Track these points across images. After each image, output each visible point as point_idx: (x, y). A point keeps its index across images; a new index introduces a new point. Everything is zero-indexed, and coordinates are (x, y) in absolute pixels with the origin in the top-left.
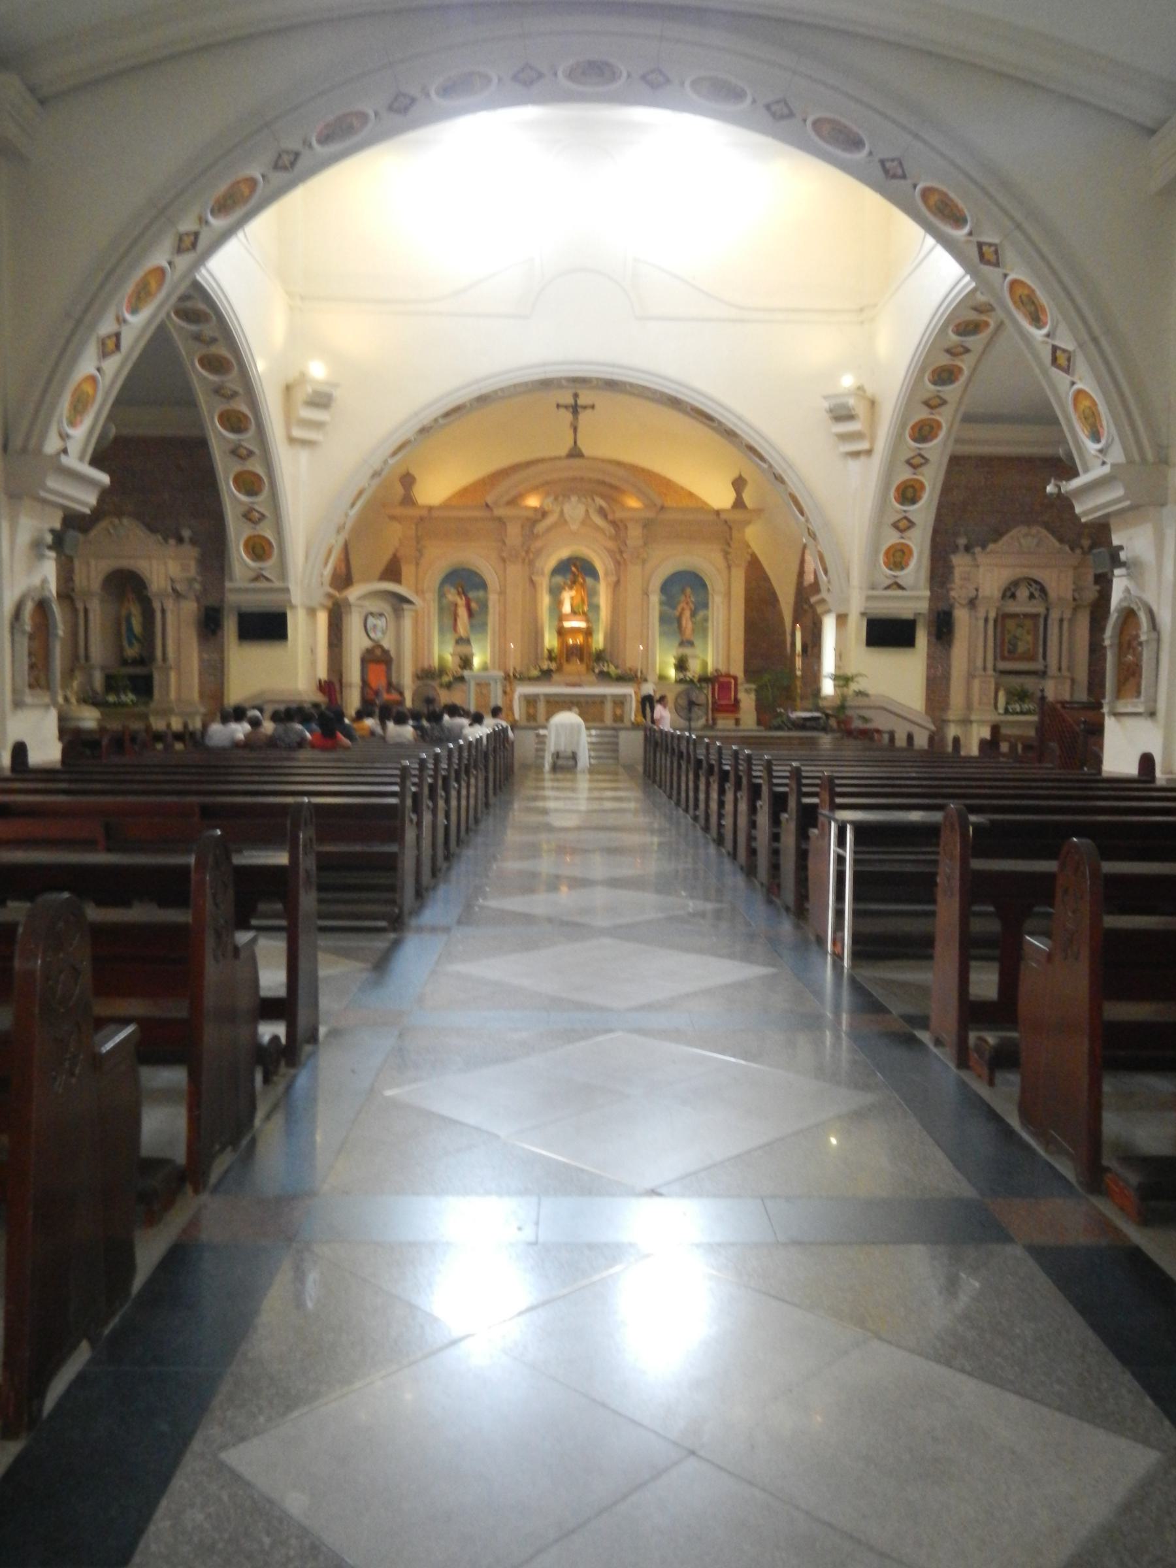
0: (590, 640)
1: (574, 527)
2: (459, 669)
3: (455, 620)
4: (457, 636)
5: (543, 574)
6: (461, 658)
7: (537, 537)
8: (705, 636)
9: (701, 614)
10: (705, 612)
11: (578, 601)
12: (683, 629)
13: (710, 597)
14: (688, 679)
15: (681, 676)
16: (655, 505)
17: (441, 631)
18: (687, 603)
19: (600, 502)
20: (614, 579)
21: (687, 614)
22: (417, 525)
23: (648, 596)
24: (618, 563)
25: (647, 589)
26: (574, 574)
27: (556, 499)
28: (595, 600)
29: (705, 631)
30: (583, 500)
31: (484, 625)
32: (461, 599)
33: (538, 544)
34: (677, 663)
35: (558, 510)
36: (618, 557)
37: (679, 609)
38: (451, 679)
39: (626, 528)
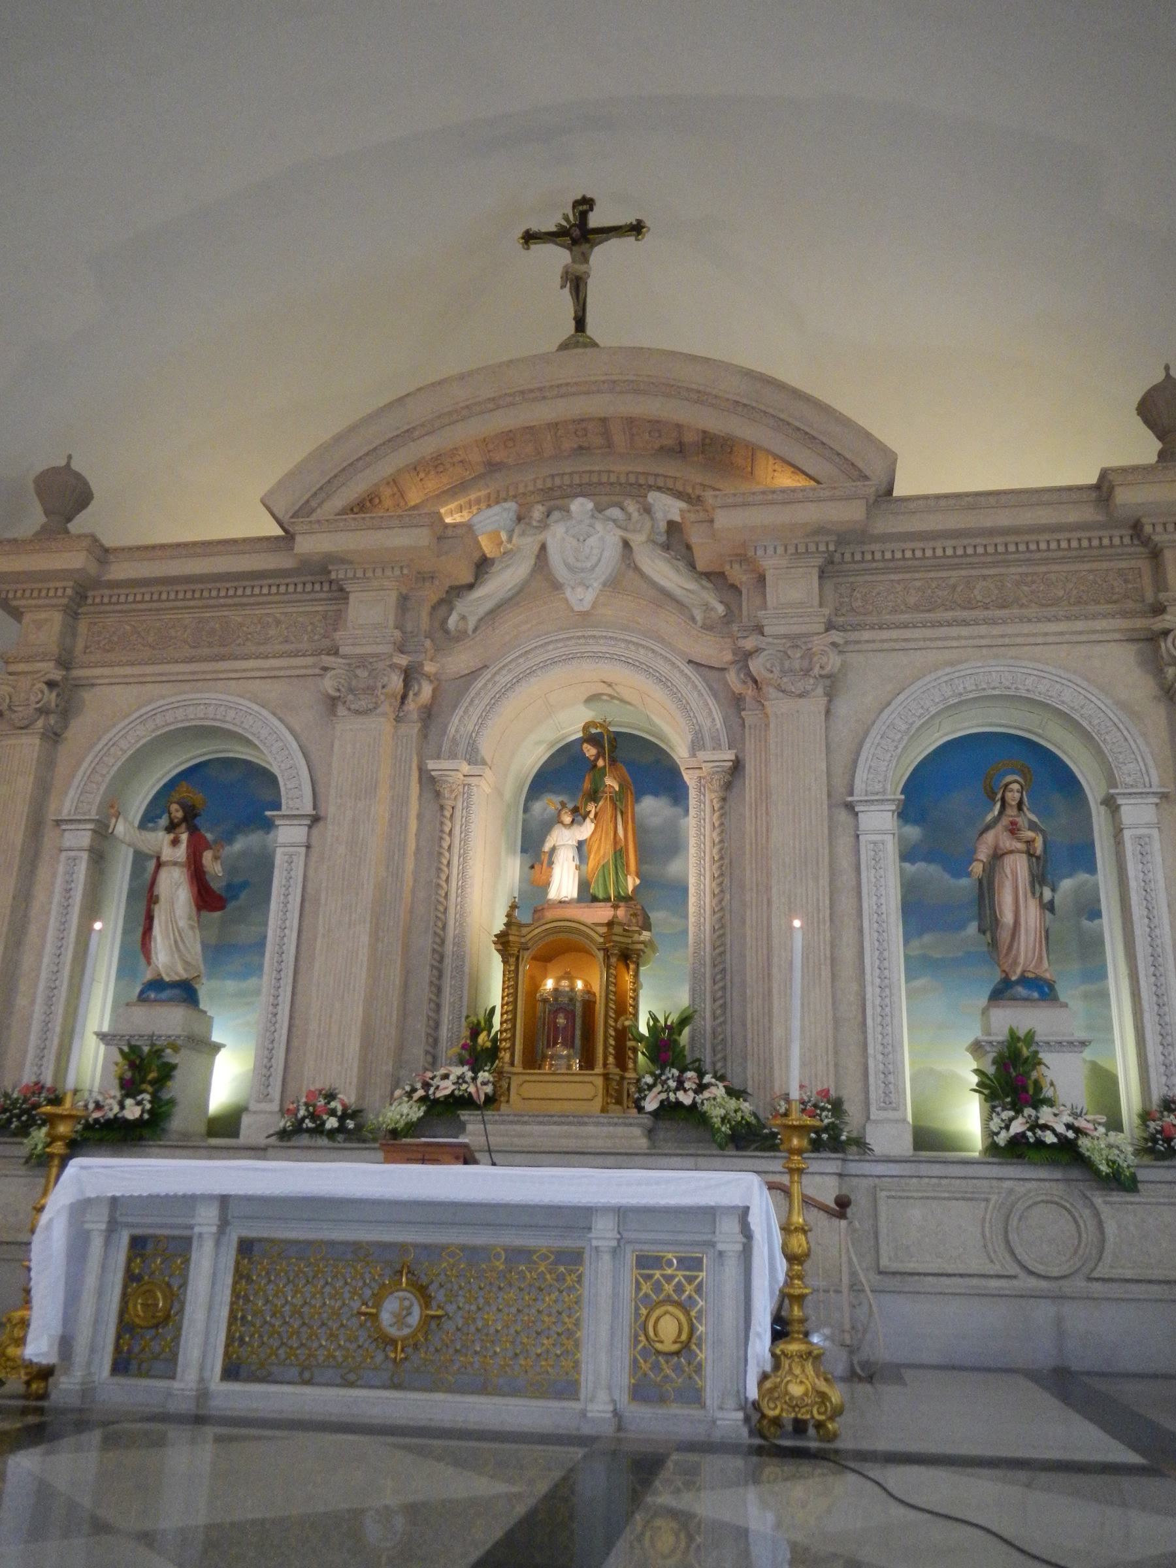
0: (628, 978)
1: (582, 598)
4: (149, 976)
5: (473, 757)
7: (461, 636)
8: (1096, 973)
9: (1066, 884)
10: (1083, 877)
11: (602, 852)
12: (1004, 936)
13: (1099, 818)
14: (1050, 1138)
15: (1017, 1127)
16: (866, 478)
17: (126, 969)
18: (1013, 830)
19: (668, 507)
20: (730, 755)
21: (1017, 868)
23: (850, 807)
25: (851, 794)
27: (519, 519)
28: (673, 868)
29: (1092, 947)
30: (615, 512)
32: (175, 842)
33: (459, 661)
34: (991, 1070)
35: (528, 544)
37: (983, 853)
39: (762, 579)
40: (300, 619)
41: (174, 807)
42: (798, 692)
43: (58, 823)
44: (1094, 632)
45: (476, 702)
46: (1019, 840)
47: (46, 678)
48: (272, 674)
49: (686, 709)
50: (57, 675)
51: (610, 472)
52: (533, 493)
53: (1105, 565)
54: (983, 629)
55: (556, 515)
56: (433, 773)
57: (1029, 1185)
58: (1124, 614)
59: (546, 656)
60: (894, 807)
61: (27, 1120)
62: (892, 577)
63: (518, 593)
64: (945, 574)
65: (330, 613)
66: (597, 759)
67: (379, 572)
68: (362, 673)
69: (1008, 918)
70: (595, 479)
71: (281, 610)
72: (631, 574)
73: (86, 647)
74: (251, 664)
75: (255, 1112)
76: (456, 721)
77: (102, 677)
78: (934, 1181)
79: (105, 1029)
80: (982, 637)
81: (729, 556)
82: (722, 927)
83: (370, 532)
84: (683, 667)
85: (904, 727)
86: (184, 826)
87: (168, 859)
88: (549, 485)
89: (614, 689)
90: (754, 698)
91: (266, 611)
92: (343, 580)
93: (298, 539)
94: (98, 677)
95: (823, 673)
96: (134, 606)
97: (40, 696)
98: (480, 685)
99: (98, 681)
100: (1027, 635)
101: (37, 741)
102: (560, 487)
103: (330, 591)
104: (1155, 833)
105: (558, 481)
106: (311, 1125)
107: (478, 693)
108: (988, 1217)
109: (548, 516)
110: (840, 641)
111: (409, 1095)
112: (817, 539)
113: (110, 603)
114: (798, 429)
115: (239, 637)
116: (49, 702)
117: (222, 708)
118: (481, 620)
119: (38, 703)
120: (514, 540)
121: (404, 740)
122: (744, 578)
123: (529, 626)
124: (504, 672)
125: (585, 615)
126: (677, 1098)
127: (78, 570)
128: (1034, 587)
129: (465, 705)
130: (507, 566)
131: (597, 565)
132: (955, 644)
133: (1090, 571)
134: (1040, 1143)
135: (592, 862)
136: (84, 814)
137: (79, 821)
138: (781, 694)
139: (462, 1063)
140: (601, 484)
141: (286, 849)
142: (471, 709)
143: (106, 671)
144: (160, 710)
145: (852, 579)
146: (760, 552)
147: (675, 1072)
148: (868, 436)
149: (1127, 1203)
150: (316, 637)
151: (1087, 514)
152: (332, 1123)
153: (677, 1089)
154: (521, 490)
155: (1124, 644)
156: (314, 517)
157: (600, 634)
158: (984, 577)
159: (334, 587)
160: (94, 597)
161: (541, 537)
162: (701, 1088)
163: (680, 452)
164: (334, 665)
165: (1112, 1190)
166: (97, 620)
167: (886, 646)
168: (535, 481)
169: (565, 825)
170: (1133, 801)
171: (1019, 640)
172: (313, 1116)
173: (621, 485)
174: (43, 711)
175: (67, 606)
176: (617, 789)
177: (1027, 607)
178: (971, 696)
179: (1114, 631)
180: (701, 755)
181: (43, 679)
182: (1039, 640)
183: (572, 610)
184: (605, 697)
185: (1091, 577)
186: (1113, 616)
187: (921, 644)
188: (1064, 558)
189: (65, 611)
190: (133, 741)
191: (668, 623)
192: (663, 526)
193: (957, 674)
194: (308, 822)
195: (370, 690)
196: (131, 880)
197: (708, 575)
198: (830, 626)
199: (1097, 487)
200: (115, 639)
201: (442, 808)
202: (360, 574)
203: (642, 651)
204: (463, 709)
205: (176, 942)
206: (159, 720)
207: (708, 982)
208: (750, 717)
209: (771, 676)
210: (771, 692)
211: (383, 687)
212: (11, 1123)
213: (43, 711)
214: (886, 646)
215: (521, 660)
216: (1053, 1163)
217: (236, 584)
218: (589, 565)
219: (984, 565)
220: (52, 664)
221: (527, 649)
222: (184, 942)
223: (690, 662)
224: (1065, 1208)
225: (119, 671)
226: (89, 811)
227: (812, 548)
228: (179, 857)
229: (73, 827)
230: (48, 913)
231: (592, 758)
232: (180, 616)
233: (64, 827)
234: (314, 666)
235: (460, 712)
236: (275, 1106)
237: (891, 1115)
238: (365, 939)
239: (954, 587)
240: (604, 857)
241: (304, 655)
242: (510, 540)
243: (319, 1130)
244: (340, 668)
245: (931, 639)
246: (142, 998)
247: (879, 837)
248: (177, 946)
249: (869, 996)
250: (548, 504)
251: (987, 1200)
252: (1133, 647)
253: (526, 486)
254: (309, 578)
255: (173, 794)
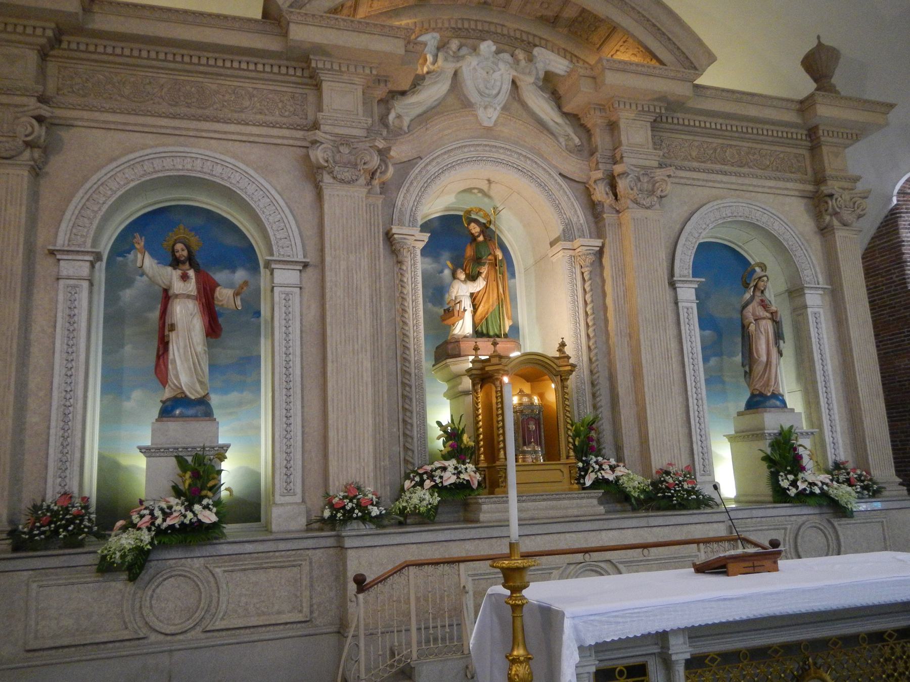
2: (178, 507)
3: (164, 345)
4: (168, 394)
6: (181, 461)
12: (758, 369)
14: (817, 491)
20: (598, 243)
22: (44, 56)
24: (594, 209)
26: (474, 238)
31: (250, 362)
32: (185, 277)
33: (401, 151)
34: (769, 451)
35: (450, 67)
36: (601, 193)
38: (146, 537)
39: (613, 126)
40: (270, 96)
41: (179, 246)
42: (648, 205)
43: (52, 253)
44: (787, 189)
45: (415, 184)
46: (767, 311)
47: (36, 113)
48: (252, 139)
49: (558, 207)
50: (45, 111)
51: (503, 25)
52: (447, 29)
53: (788, 150)
54: (733, 179)
55: (464, 51)
56: (396, 236)
57: (805, 518)
58: (802, 182)
59: (462, 156)
60: (697, 286)
61: (74, 528)
62: (683, 137)
63: (438, 105)
64: (710, 140)
65: (297, 95)
66: (478, 236)
67: (352, 69)
68: (345, 150)
69: (764, 358)
70: (493, 28)
71: (254, 86)
72: (516, 104)
73: (58, 89)
74: (232, 128)
75: (282, 505)
76: (402, 198)
77: (82, 119)
78: (759, 519)
79: (148, 443)
80: (732, 183)
81: (595, 104)
82: (597, 360)
83: (356, 34)
84: (557, 178)
85: (697, 235)
86: (188, 263)
87: (181, 292)
88: (460, 26)
89: (489, 187)
90: (611, 206)
91: (241, 84)
92: (321, 69)
93: (292, 27)
94: (76, 119)
95: (663, 194)
96: (111, 58)
97: (30, 129)
98: (417, 171)
99: (76, 123)
100: (755, 186)
101: (26, 173)
102: (467, 29)
103: (303, 77)
104: (821, 311)
105: (466, 25)
106: (360, 514)
107: (416, 178)
108: (787, 539)
109: (459, 50)
110: (672, 175)
111: (421, 483)
112: (656, 103)
113: (86, 51)
114: (654, 25)
115: (215, 103)
116: (39, 137)
117: (209, 163)
118: (411, 120)
119: (26, 136)
120: (440, 62)
121: (372, 207)
122: (599, 121)
123: (450, 131)
124: (434, 163)
125: (489, 129)
126: (603, 477)
127: (70, 14)
128: (755, 156)
129: (407, 185)
130: (435, 83)
131: (499, 93)
132: (719, 185)
133: (782, 152)
134: (812, 494)
135: (480, 310)
136: (79, 245)
137: (78, 252)
138: (635, 205)
139: (446, 457)
140: (496, 33)
141: (283, 289)
142: (412, 189)
143: (86, 114)
144: (147, 157)
145: (661, 134)
146: (622, 106)
147: (594, 459)
148: (699, 41)
149: (848, 524)
150: (287, 114)
151: (791, 117)
152: (375, 511)
153: (599, 470)
154: (440, 25)
155: (800, 198)
156: (303, 11)
157: (500, 145)
158: (731, 146)
159: (306, 73)
160: (69, 42)
161: (458, 65)
162: (612, 468)
163: (553, 23)
164: (323, 140)
165: (840, 517)
166: (68, 65)
167: (683, 181)
168: (449, 20)
169: (461, 281)
170: (812, 292)
171: (751, 188)
172: (359, 505)
173: (509, 37)
174: (28, 144)
175: (43, 47)
176: (500, 258)
177: (752, 168)
178: (729, 220)
179: (796, 190)
180: (578, 242)
181: (31, 113)
182: (760, 190)
183: (480, 124)
184: (476, 191)
185: (782, 156)
186: (796, 181)
187: (700, 183)
188: (772, 142)
189: (39, 51)
190: (122, 183)
191: (546, 145)
192: (541, 75)
193: (722, 205)
194: (301, 268)
195: (355, 166)
196: (106, 305)
197: (566, 115)
198: (661, 166)
199: (801, 102)
200: (90, 85)
201: (400, 262)
202: (336, 67)
203: (529, 162)
204: (405, 188)
205: (194, 364)
206: (147, 167)
207: (588, 397)
208: (609, 217)
209: (631, 192)
210: (625, 202)
211: (365, 164)
212: (58, 534)
213: (28, 144)
214: (683, 181)
215: (446, 156)
216: (820, 506)
217: (217, 55)
218: (494, 92)
219: (732, 138)
220: (32, 102)
221: (450, 148)
222: (200, 365)
223: (560, 174)
224: (821, 530)
225: (97, 115)
226: (85, 242)
227: (652, 109)
228: (192, 291)
229: (70, 257)
230: (53, 336)
231: (476, 234)
232: (155, 75)
233: (59, 257)
234: (304, 139)
235: (403, 190)
236: (298, 498)
237: (707, 478)
238: (367, 364)
239: (715, 150)
240: (493, 305)
241: (281, 127)
242: (435, 62)
243: (366, 518)
244: (327, 143)
245: (706, 181)
246: (166, 412)
247: (689, 305)
248: (195, 370)
249: (691, 405)
250: (463, 41)
251: (785, 529)
252: (806, 200)
253: (443, 23)
254: (285, 62)
255: (170, 234)
